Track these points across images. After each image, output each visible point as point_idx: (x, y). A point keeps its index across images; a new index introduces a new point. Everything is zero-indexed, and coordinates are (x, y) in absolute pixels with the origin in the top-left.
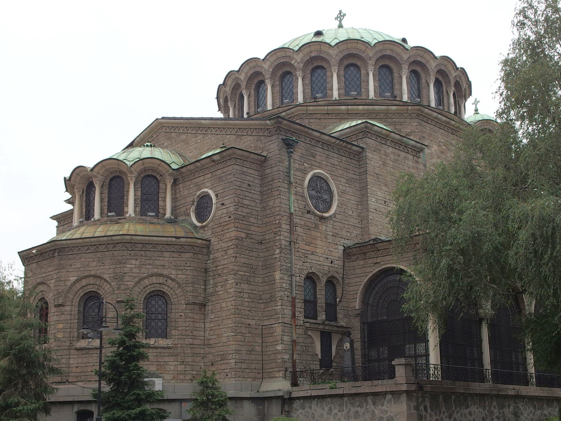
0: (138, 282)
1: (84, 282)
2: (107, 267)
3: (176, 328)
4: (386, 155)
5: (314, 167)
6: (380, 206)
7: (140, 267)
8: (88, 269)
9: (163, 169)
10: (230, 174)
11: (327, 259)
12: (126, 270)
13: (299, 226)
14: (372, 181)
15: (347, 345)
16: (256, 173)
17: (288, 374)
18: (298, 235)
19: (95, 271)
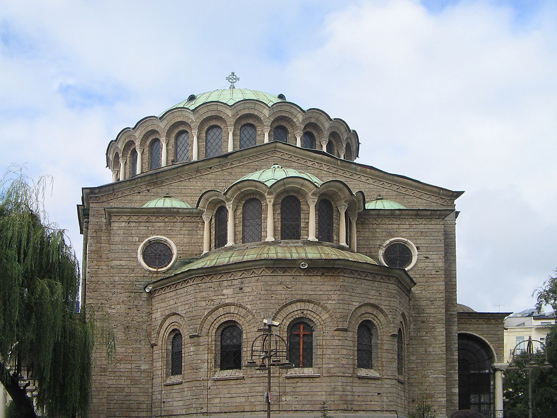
1: (363, 310)
19: (374, 300)
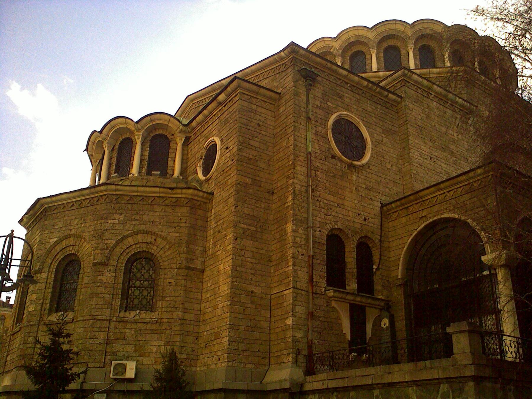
2: (88, 224)
3: (163, 299)
4: (430, 109)
5: (341, 109)
6: (425, 161)
7: (124, 223)
8: (69, 227)
10: (235, 112)
11: (359, 214)
13: (320, 170)
14: (414, 133)
15: (385, 322)
16: (269, 113)
17: (301, 358)
18: (319, 181)
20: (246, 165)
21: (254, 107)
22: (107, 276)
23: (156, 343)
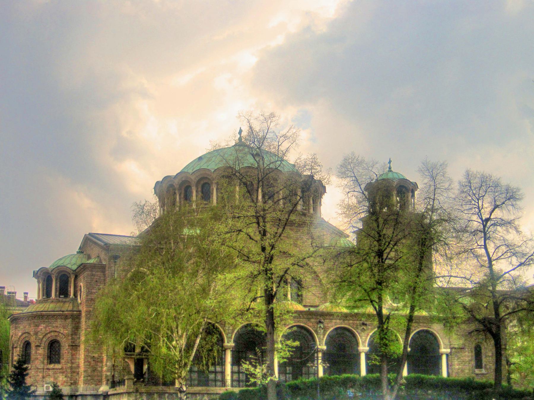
0: (45, 335)
1: (24, 336)
3: (63, 359)
7: (45, 328)
9: (69, 271)
12: (39, 330)
17: (109, 382)
20: (90, 302)
21: (94, 273)
22: (41, 351)
23: (62, 377)
